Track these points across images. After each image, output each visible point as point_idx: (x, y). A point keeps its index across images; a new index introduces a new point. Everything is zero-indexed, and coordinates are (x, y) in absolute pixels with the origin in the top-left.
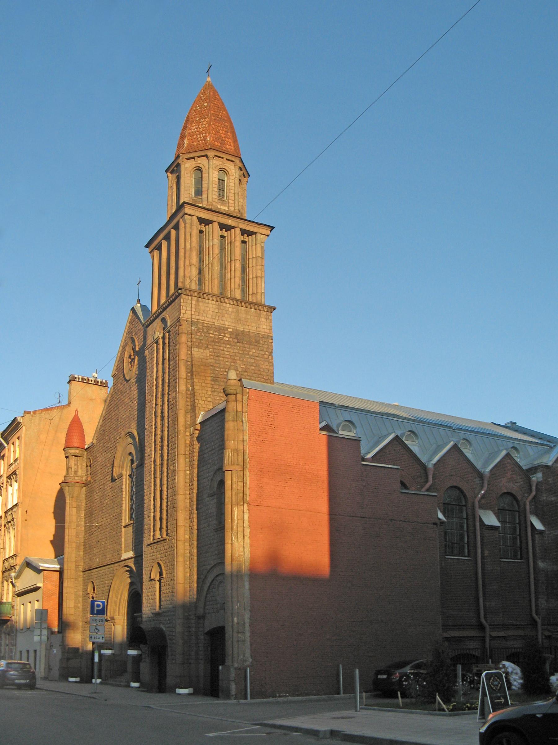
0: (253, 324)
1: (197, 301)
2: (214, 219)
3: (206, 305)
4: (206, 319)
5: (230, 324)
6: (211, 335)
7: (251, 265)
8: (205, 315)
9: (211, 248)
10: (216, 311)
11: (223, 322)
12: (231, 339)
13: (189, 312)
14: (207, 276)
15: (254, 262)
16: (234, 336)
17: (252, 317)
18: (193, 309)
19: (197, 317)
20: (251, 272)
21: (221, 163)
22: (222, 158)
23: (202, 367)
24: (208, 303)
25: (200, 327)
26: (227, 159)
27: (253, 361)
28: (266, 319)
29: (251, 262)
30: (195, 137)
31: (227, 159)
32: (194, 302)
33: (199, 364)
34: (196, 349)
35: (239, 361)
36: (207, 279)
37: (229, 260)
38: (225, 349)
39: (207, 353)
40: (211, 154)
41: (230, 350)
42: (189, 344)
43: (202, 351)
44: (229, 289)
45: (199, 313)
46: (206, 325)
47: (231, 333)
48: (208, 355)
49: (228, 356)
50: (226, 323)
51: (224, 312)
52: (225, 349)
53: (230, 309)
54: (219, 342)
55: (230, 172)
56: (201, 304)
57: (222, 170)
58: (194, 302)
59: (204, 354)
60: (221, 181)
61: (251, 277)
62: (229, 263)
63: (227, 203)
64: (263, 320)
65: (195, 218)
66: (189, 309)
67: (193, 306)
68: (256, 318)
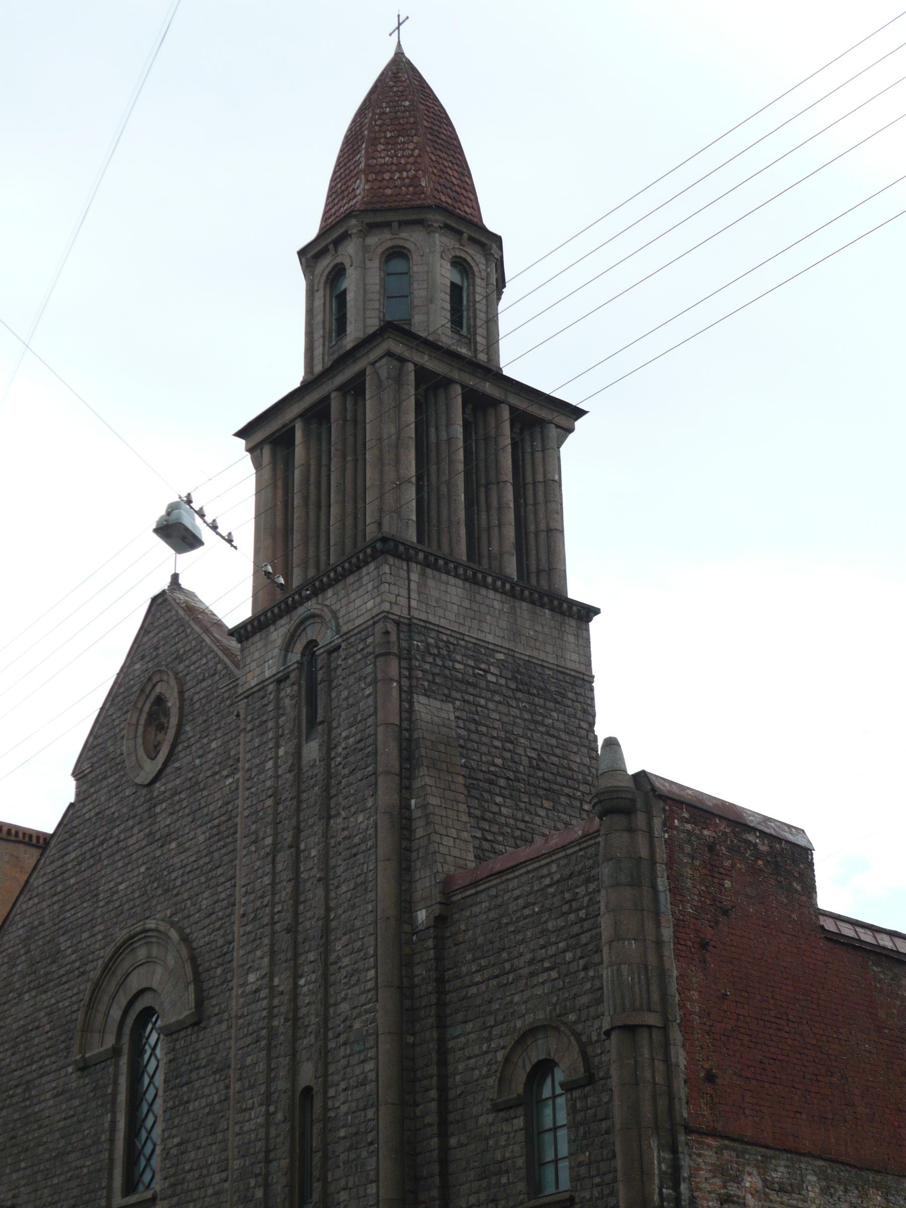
0: (549, 648)
1: (423, 575)
2: (455, 375)
3: (443, 587)
4: (443, 623)
5: (498, 641)
6: (458, 666)
7: (530, 501)
8: (440, 612)
9: (444, 446)
10: (466, 604)
11: (481, 636)
12: (502, 681)
13: (403, 601)
14: (434, 514)
15: (541, 494)
16: (509, 675)
17: (546, 630)
18: (414, 595)
19: (423, 616)
20: (531, 517)
21: (458, 245)
22: (460, 233)
23: (442, 748)
24: (448, 584)
25: (432, 641)
26: (471, 239)
27: (553, 742)
28: (577, 636)
29: (530, 493)
30: (387, 176)
31: (471, 239)
32: (414, 577)
33: (433, 738)
34: (423, 699)
35: (522, 740)
36: (434, 521)
37: (483, 481)
38: (491, 705)
39: (448, 712)
40: (436, 219)
41: (502, 708)
42: (405, 682)
43: (438, 704)
44: (485, 553)
45: (427, 604)
46: (445, 638)
47: (501, 664)
48: (452, 717)
49: (497, 724)
50: (490, 638)
51: (484, 609)
52: (491, 705)
53: (496, 604)
54: (475, 686)
55: (476, 269)
56: (431, 583)
57: (460, 264)
58: (414, 577)
59: (444, 715)
60: (456, 290)
61: (532, 528)
62: (483, 489)
63: (471, 342)
64: (571, 639)
65: (411, 367)
66: (404, 593)
67: (413, 586)
68: (556, 633)
